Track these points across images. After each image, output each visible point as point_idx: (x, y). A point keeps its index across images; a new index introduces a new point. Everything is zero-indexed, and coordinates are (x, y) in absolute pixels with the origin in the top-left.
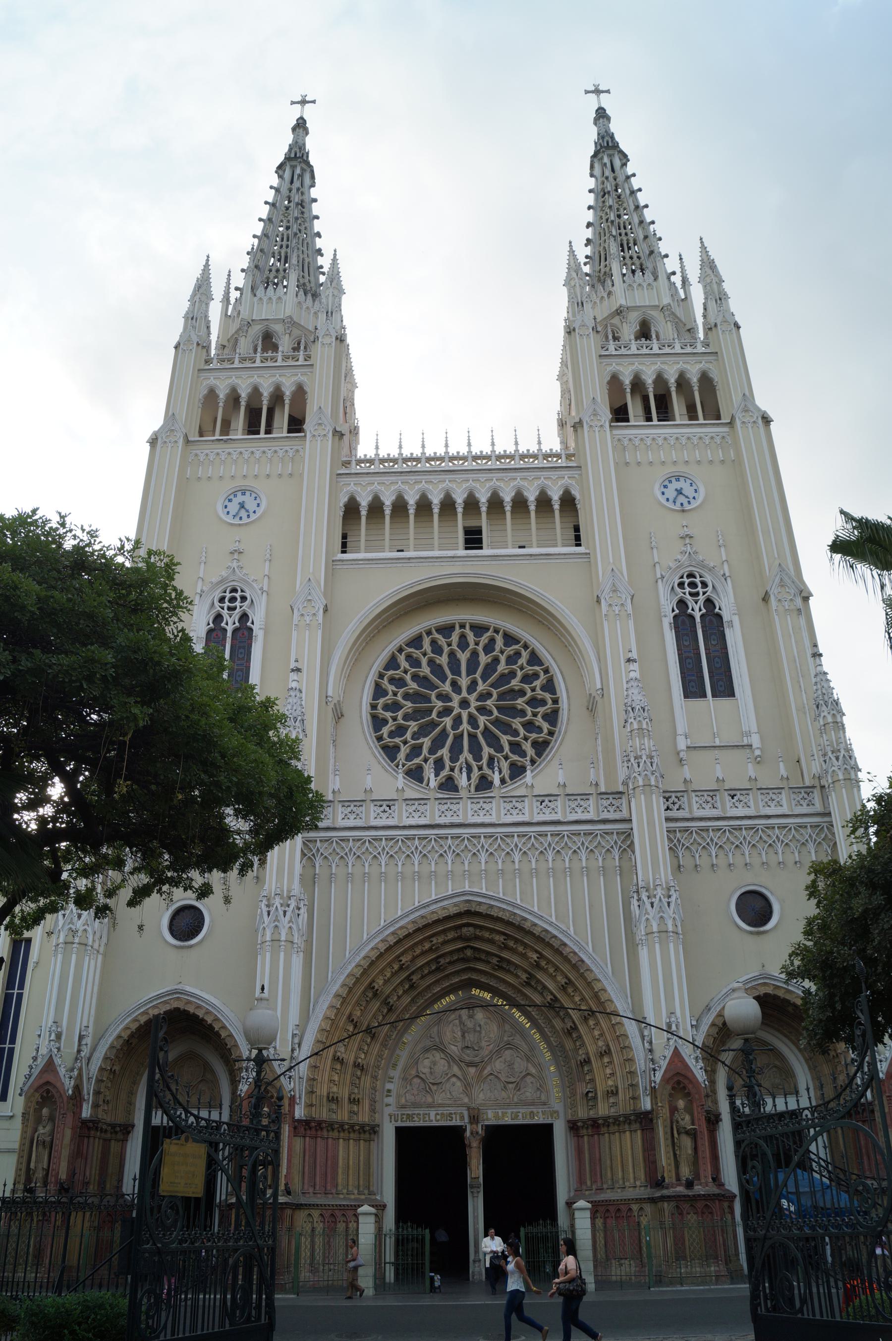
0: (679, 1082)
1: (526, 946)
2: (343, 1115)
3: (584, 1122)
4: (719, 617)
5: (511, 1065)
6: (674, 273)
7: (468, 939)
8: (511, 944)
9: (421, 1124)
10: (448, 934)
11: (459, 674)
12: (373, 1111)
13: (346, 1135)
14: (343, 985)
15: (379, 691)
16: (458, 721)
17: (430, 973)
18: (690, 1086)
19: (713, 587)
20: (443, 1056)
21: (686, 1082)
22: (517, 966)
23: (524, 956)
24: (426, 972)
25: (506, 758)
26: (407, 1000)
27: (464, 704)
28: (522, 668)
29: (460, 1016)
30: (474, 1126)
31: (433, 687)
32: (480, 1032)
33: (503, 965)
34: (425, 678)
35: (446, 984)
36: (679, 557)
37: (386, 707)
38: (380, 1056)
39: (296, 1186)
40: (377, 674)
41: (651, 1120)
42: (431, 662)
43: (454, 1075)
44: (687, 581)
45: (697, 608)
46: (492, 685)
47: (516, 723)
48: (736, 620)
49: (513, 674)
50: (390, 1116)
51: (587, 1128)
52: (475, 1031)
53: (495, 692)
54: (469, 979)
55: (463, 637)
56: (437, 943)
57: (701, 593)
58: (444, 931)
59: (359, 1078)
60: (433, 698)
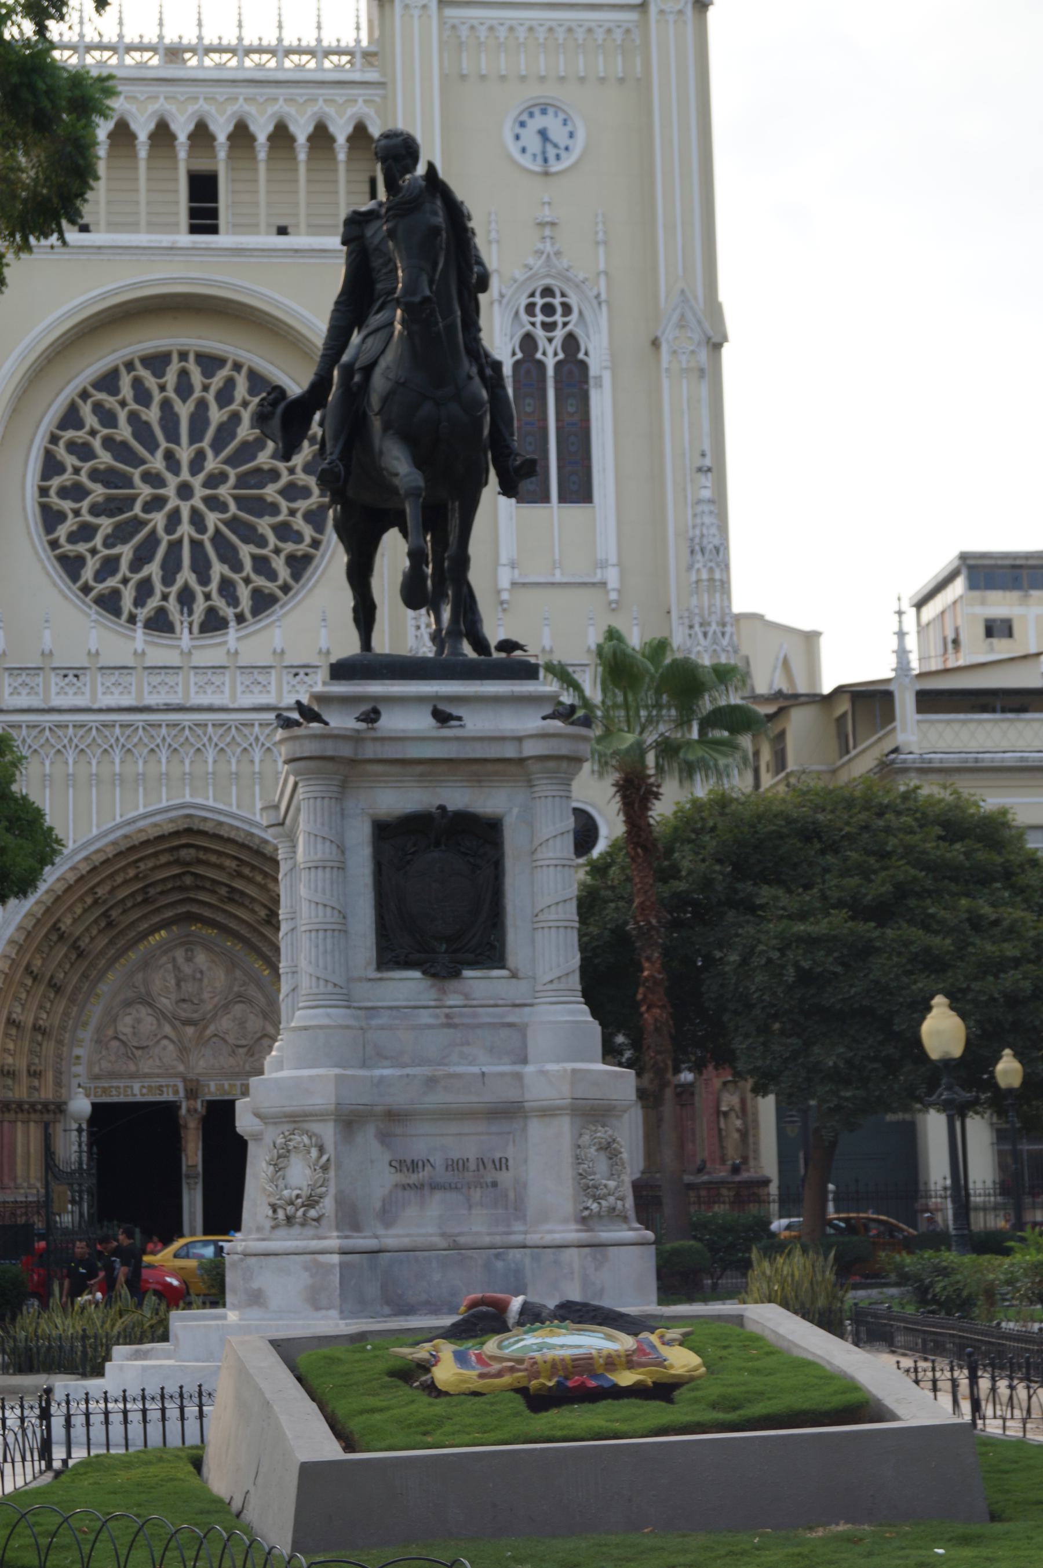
4: (583, 366)
5: (242, 1023)
8: (246, 871)
9: (122, 1099)
11: (178, 443)
12: (58, 1084)
14: (20, 928)
15: (51, 466)
16: (174, 519)
19: (581, 313)
20: (150, 1011)
22: (253, 900)
25: (247, 581)
27: (185, 491)
29: (174, 960)
30: (192, 1102)
32: (201, 980)
33: (234, 896)
34: (124, 444)
35: (156, 919)
36: (531, 261)
37: (64, 492)
38: (66, 1014)
40: (47, 438)
42: (133, 418)
43: (166, 1037)
44: (540, 301)
45: (550, 352)
46: (227, 461)
47: (264, 525)
48: (607, 377)
52: (194, 979)
53: (232, 473)
54: (188, 912)
55: (184, 374)
57: (560, 325)
58: (155, 855)
59: (40, 1045)
60: (137, 480)
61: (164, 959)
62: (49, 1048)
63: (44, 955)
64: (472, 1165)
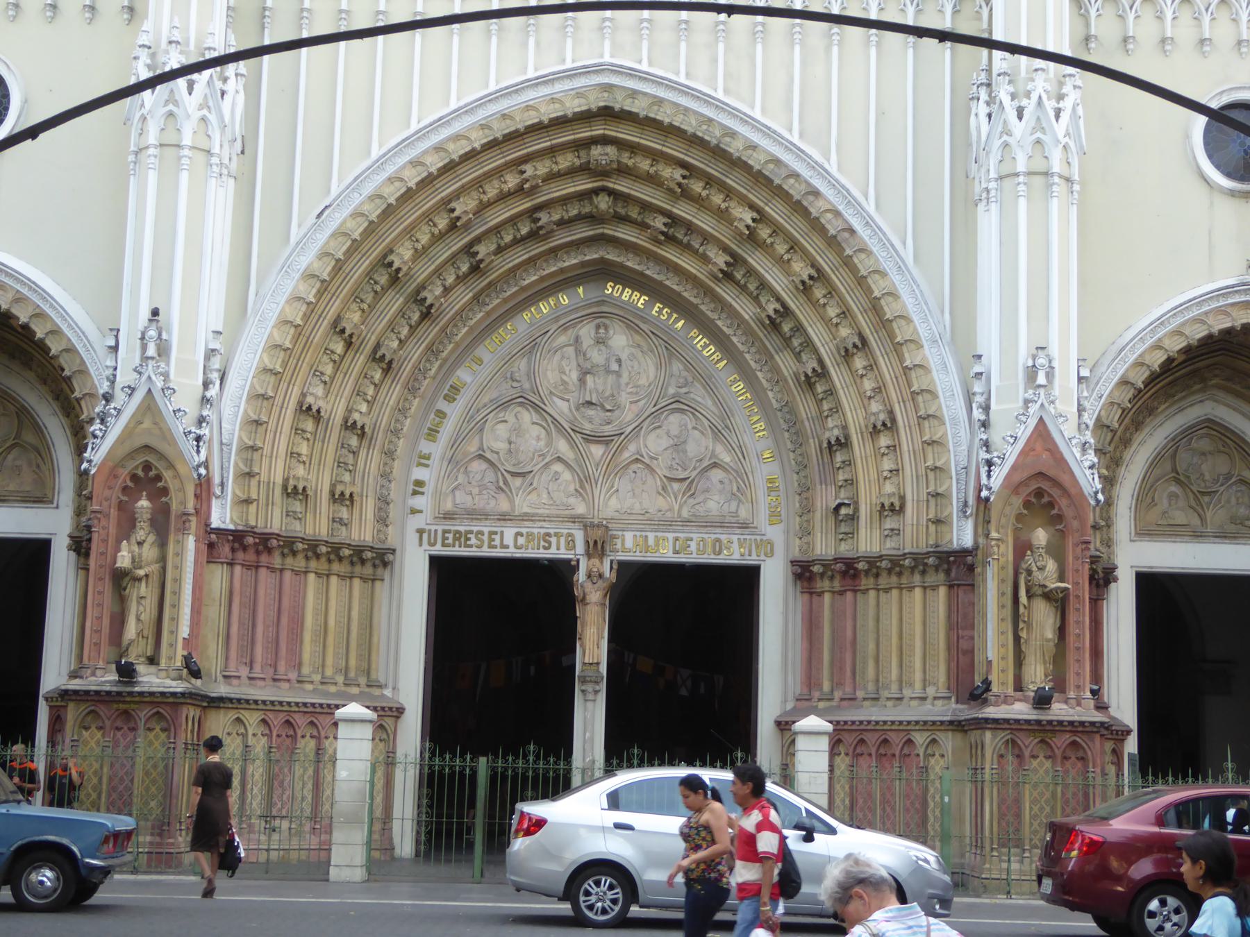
0: (1039, 493)
1: (729, 193)
2: (317, 525)
3: (826, 565)
5: (678, 446)
7: (604, 173)
8: (697, 187)
9: (486, 552)
10: (560, 159)
12: (382, 520)
13: (322, 565)
14: (324, 254)
17: (516, 242)
18: (1063, 502)
20: (536, 418)
21: (1055, 492)
22: (706, 238)
23: (722, 215)
24: (508, 238)
26: (463, 296)
30: (596, 561)
32: (618, 374)
38: (402, 411)
39: (211, 660)
41: (971, 568)
43: (559, 459)
50: (420, 532)
51: (832, 578)
52: (608, 371)
54: (602, 260)
56: (535, 177)
58: (552, 151)
61: (562, 339)
62: (371, 461)
63: (365, 306)
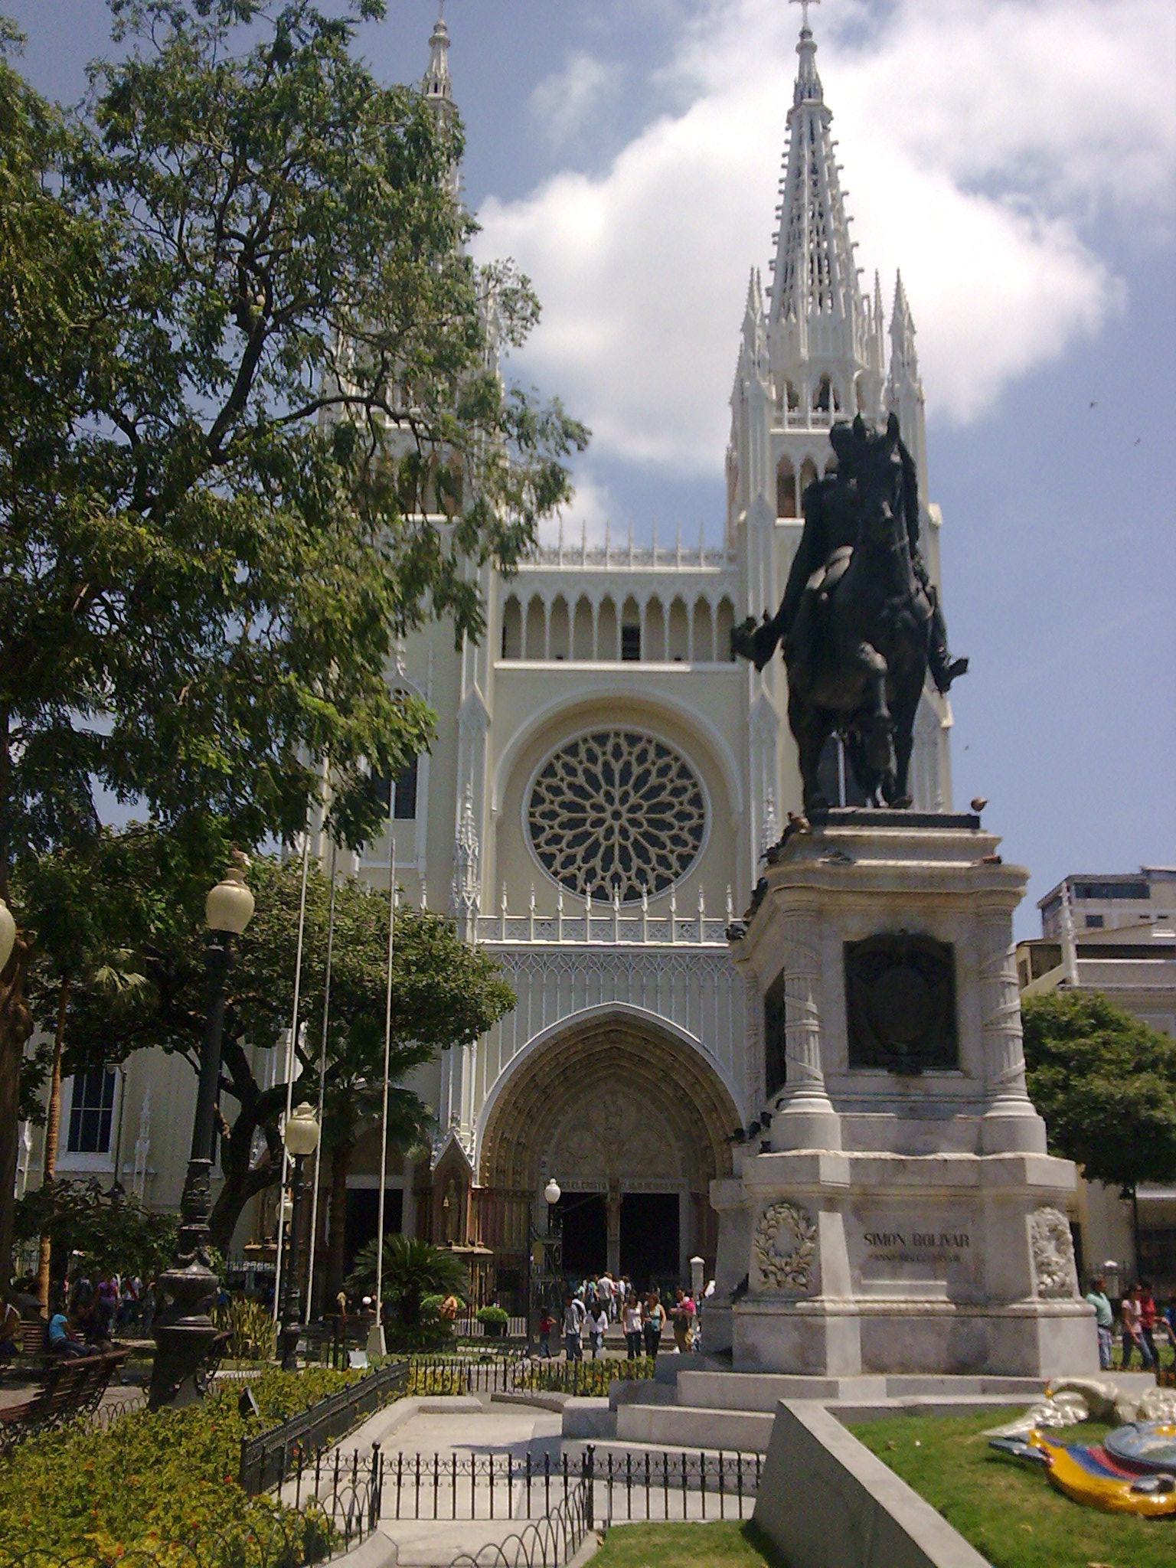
2: (509, 1184)
6: (867, 297)
15: (537, 799)
16: (609, 832)
27: (616, 815)
28: (672, 781)
31: (589, 797)
49: (662, 787)
64: (937, 1241)
